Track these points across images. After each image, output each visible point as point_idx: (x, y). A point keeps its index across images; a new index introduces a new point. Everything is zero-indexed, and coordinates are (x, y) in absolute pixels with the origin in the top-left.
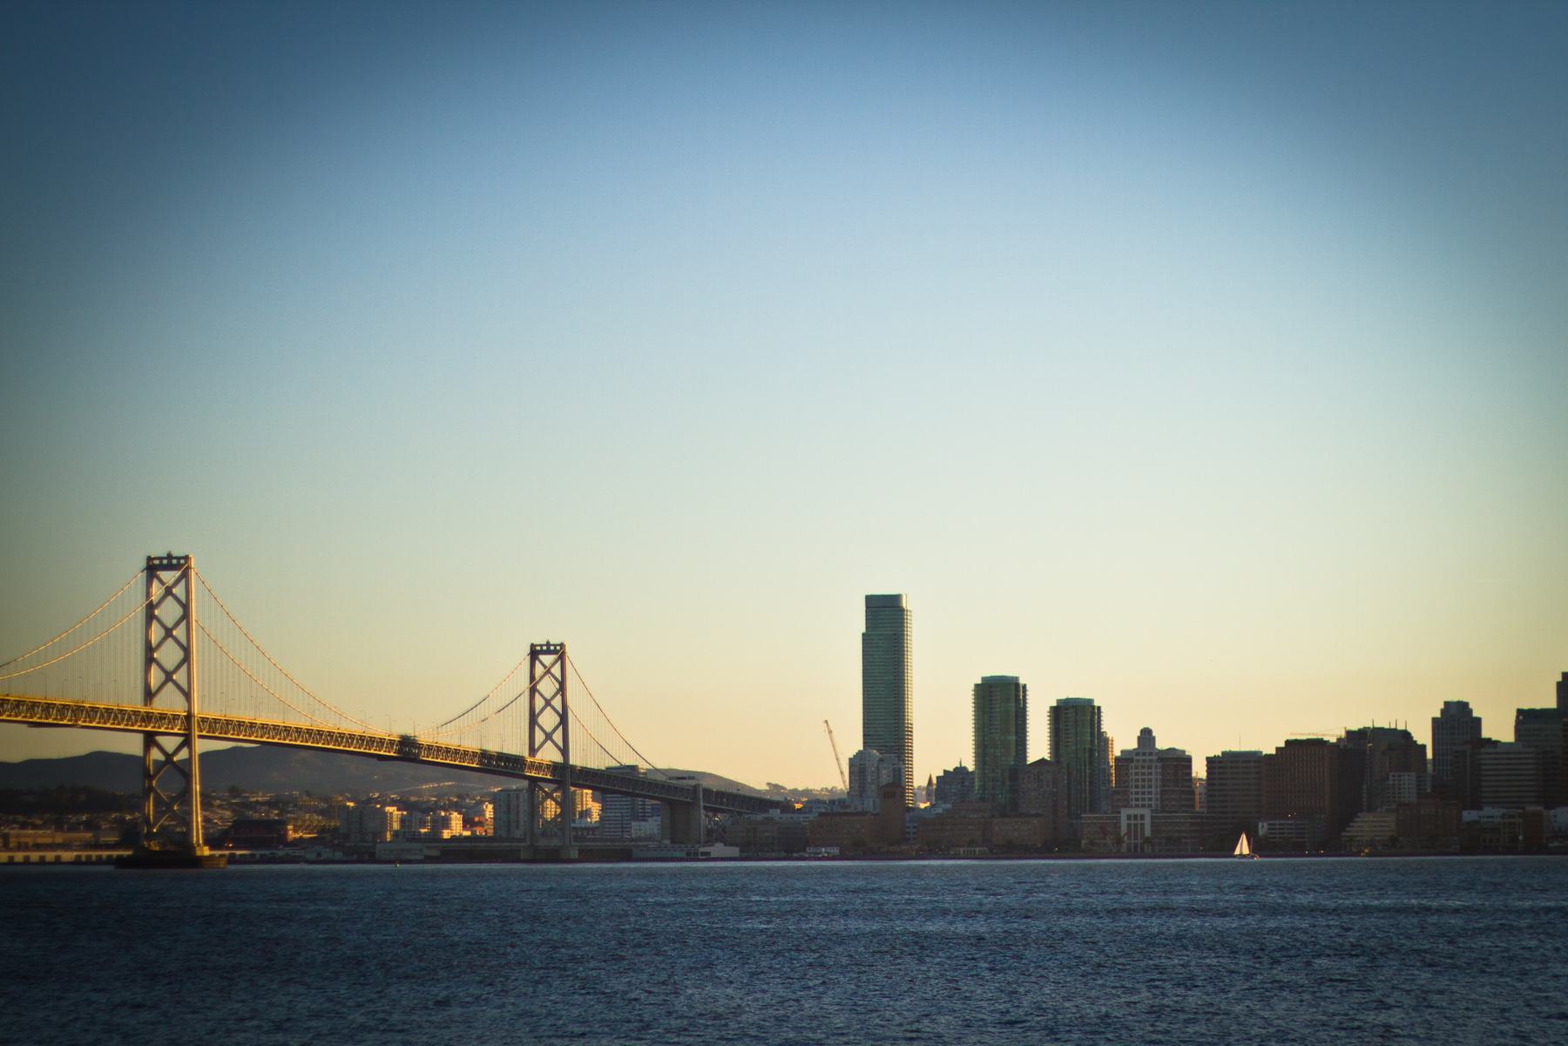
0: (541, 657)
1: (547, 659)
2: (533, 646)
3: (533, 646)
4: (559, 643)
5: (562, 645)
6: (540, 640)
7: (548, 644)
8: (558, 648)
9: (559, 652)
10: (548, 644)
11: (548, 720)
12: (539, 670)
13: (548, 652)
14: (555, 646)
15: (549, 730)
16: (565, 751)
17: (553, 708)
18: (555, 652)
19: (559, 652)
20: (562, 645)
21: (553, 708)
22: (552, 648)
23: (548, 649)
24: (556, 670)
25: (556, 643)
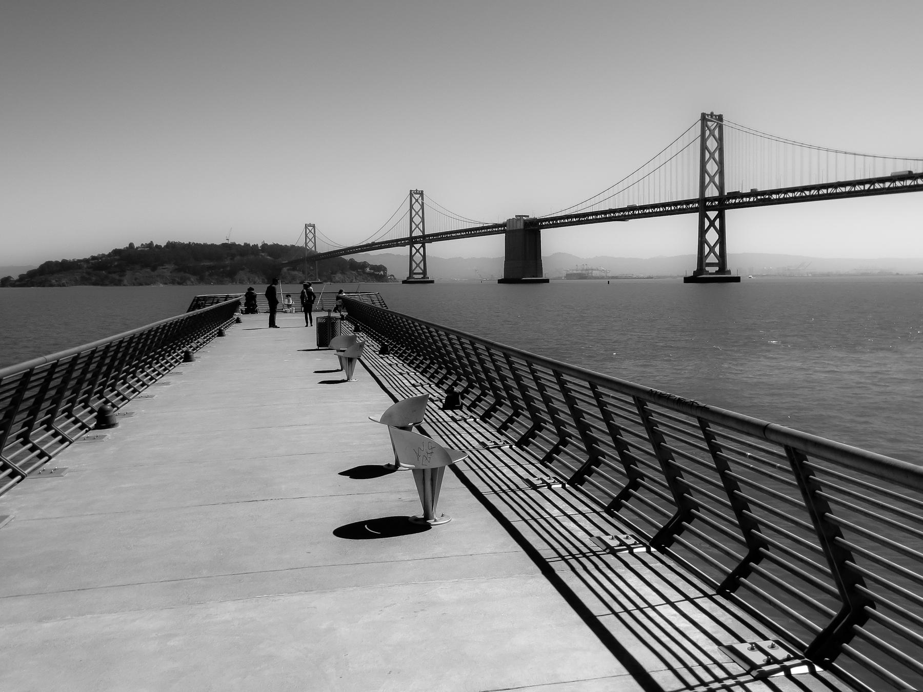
0: (414, 195)
1: (417, 196)
2: (411, 191)
5: (422, 191)
11: (417, 220)
12: (414, 200)
16: (721, 188)
18: (419, 194)
19: (421, 194)
20: (422, 191)
23: (417, 192)
24: (420, 201)
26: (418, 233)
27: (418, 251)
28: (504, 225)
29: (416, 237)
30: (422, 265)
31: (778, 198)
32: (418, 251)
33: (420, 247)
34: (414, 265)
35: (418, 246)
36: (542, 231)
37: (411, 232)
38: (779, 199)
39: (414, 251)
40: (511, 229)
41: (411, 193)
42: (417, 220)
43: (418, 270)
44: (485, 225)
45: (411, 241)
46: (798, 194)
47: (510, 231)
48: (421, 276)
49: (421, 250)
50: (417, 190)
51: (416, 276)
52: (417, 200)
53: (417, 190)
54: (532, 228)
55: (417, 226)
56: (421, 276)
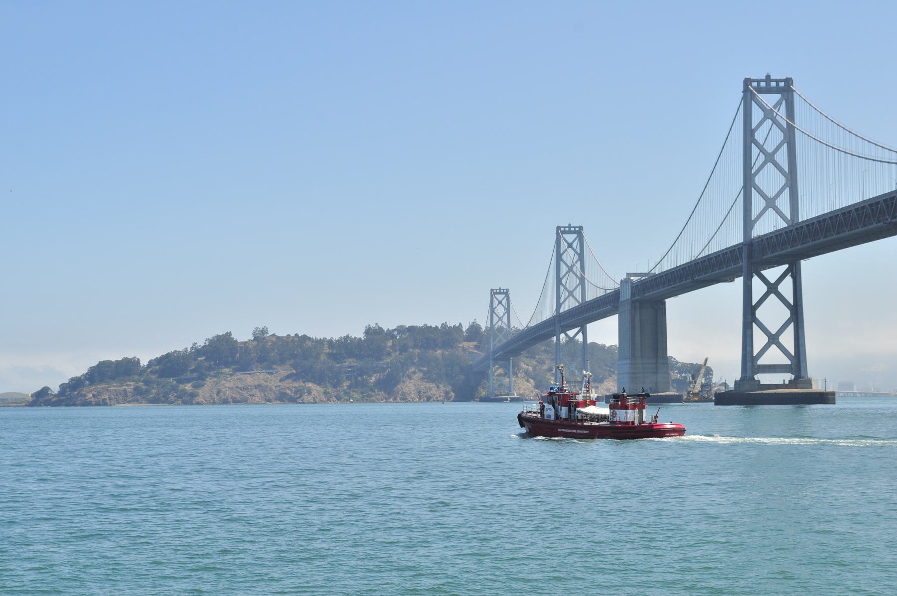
0: (761, 97)
1: (770, 100)
2: (747, 82)
3: (747, 82)
4: (784, 77)
5: (788, 81)
6: (758, 74)
7: (768, 79)
8: (782, 84)
9: (786, 89)
10: (768, 79)
12: (757, 114)
13: (768, 90)
14: (777, 81)
15: (771, 194)
17: (776, 165)
18: (776, 90)
19: (786, 89)
20: (788, 81)
21: (776, 165)
22: (773, 84)
23: (768, 86)
25: (778, 78)
27: (772, 288)
30: (788, 339)
34: (759, 339)
35: (773, 274)
37: (748, 223)
39: (758, 288)
41: (746, 90)
43: (774, 356)
48: (788, 377)
49: (787, 287)
50: (768, 77)
51: (764, 379)
52: (769, 114)
53: (768, 77)
55: (770, 203)
56: (788, 377)
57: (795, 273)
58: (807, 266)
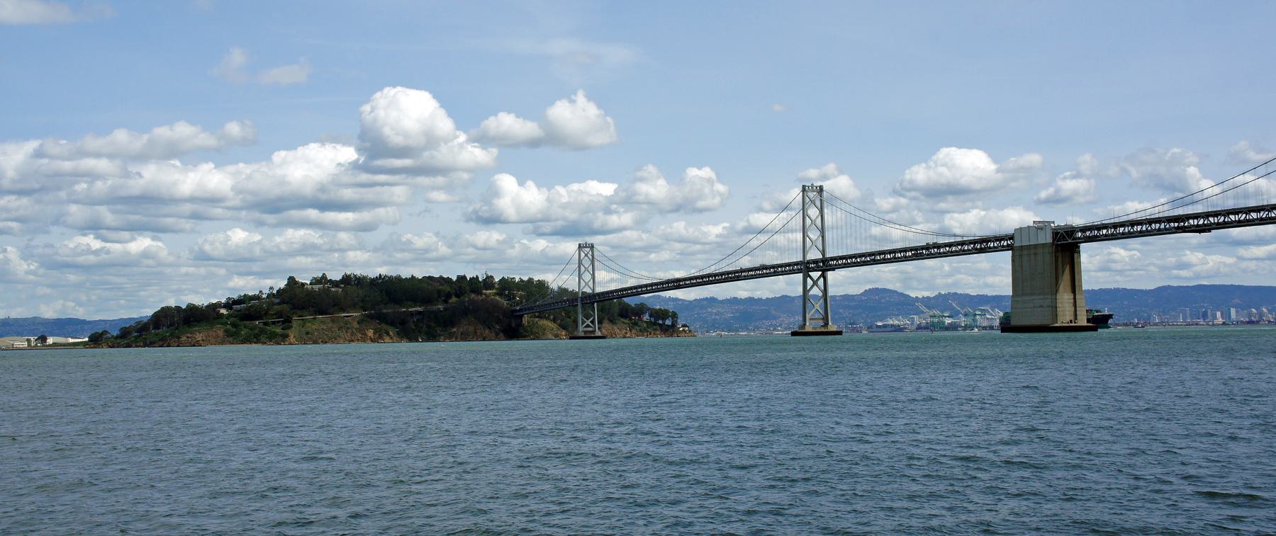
0: (811, 195)
24: (818, 204)
26: (814, 255)
27: (815, 283)
28: (1011, 238)
29: (815, 262)
31: (1237, 219)
32: (815, 283)
33: (819, 278)
35: (815, 275)
36: (1084, 247)
38: (1239, 221)
39: (809, 282)
40: (1025, 243)
42: (814, 235)
44: (965, 239)
45: (804, 267)
46: (1263, 214)
47: (1022, 247)
54: (1070, 241)
57: (824, 276)
58: (830, 274)
